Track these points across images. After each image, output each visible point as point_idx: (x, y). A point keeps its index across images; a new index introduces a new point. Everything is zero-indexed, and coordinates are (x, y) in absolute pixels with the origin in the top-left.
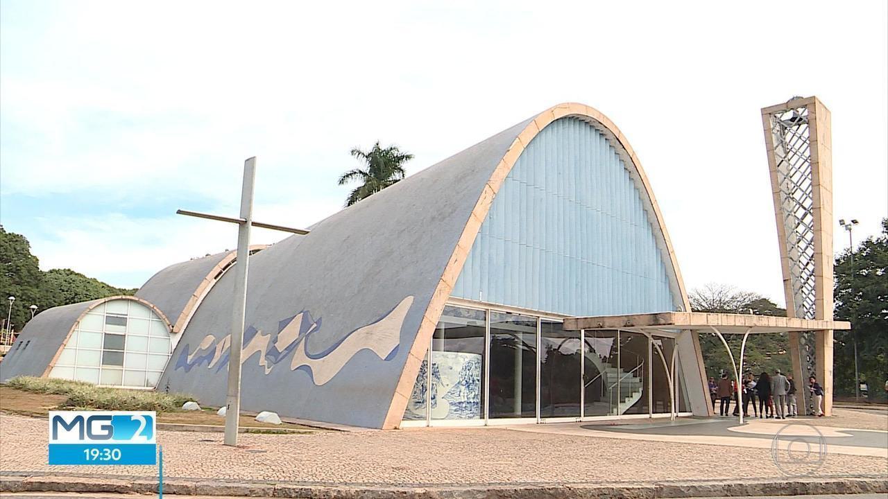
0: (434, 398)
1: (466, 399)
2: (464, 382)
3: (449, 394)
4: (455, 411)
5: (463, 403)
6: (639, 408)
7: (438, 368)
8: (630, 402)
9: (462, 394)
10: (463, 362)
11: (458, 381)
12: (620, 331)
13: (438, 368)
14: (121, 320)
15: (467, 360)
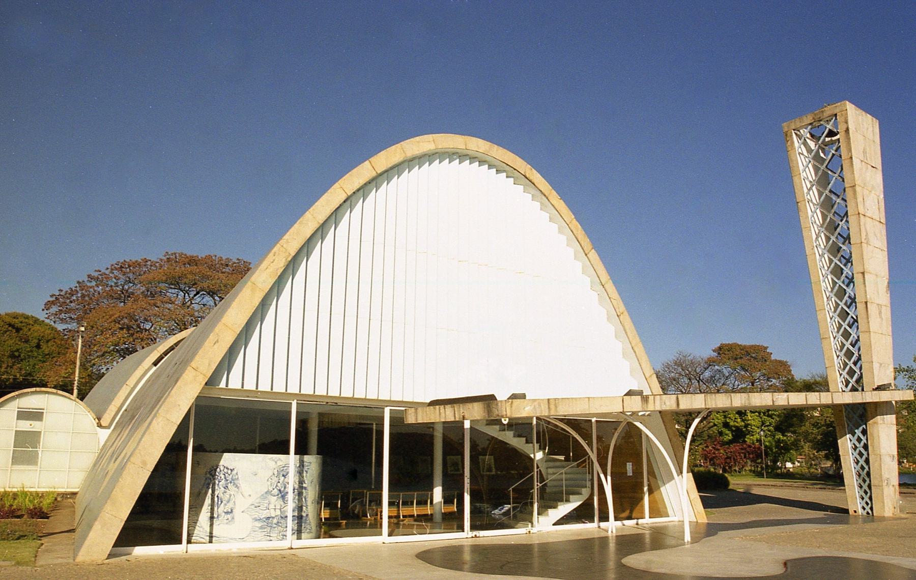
0: (232, 511)
1: (278, 512)
2: (276, 492)
3: (253, 507)
4: (261, 528)
5: (273, 518)
6: (582, 514)
7: (237, 474)
8: (565, 509)
9: (272, 506)
10: (274, 467)
11: (266, 490)
12: (14, 447)
13: (237, 474)
14: (36, 415)
15: (279, 463)
